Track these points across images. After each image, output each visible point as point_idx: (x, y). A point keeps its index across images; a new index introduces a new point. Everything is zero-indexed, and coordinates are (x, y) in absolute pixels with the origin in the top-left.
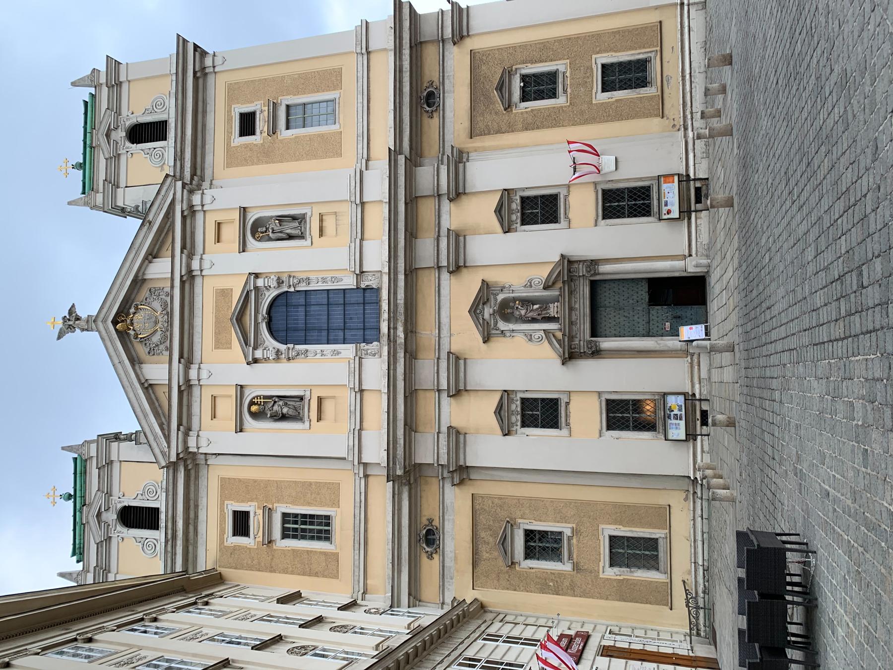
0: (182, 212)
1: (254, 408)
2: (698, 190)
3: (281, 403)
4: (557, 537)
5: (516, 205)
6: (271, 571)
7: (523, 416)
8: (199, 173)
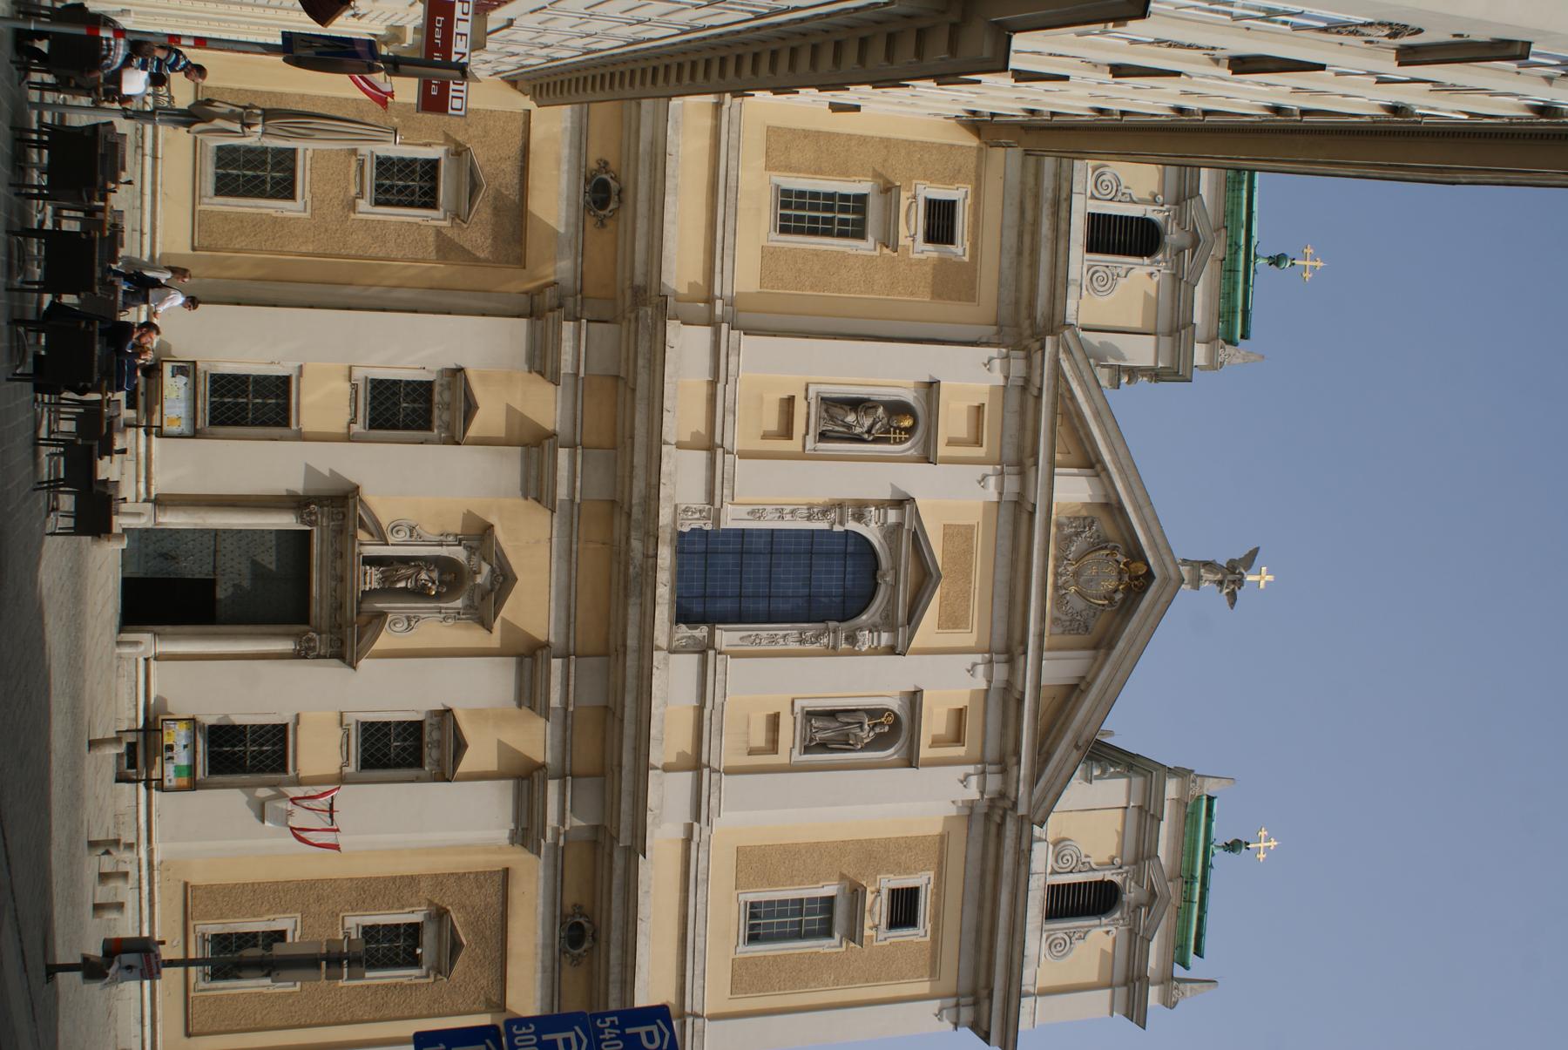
0: (1019, 763)
1: (907, 423)
2: (132, 764)
3: (858, 430)
4: (384, 197)
5: (430, 755)
6: (888, 139)
7: (429, 400)
8: (993, 829)
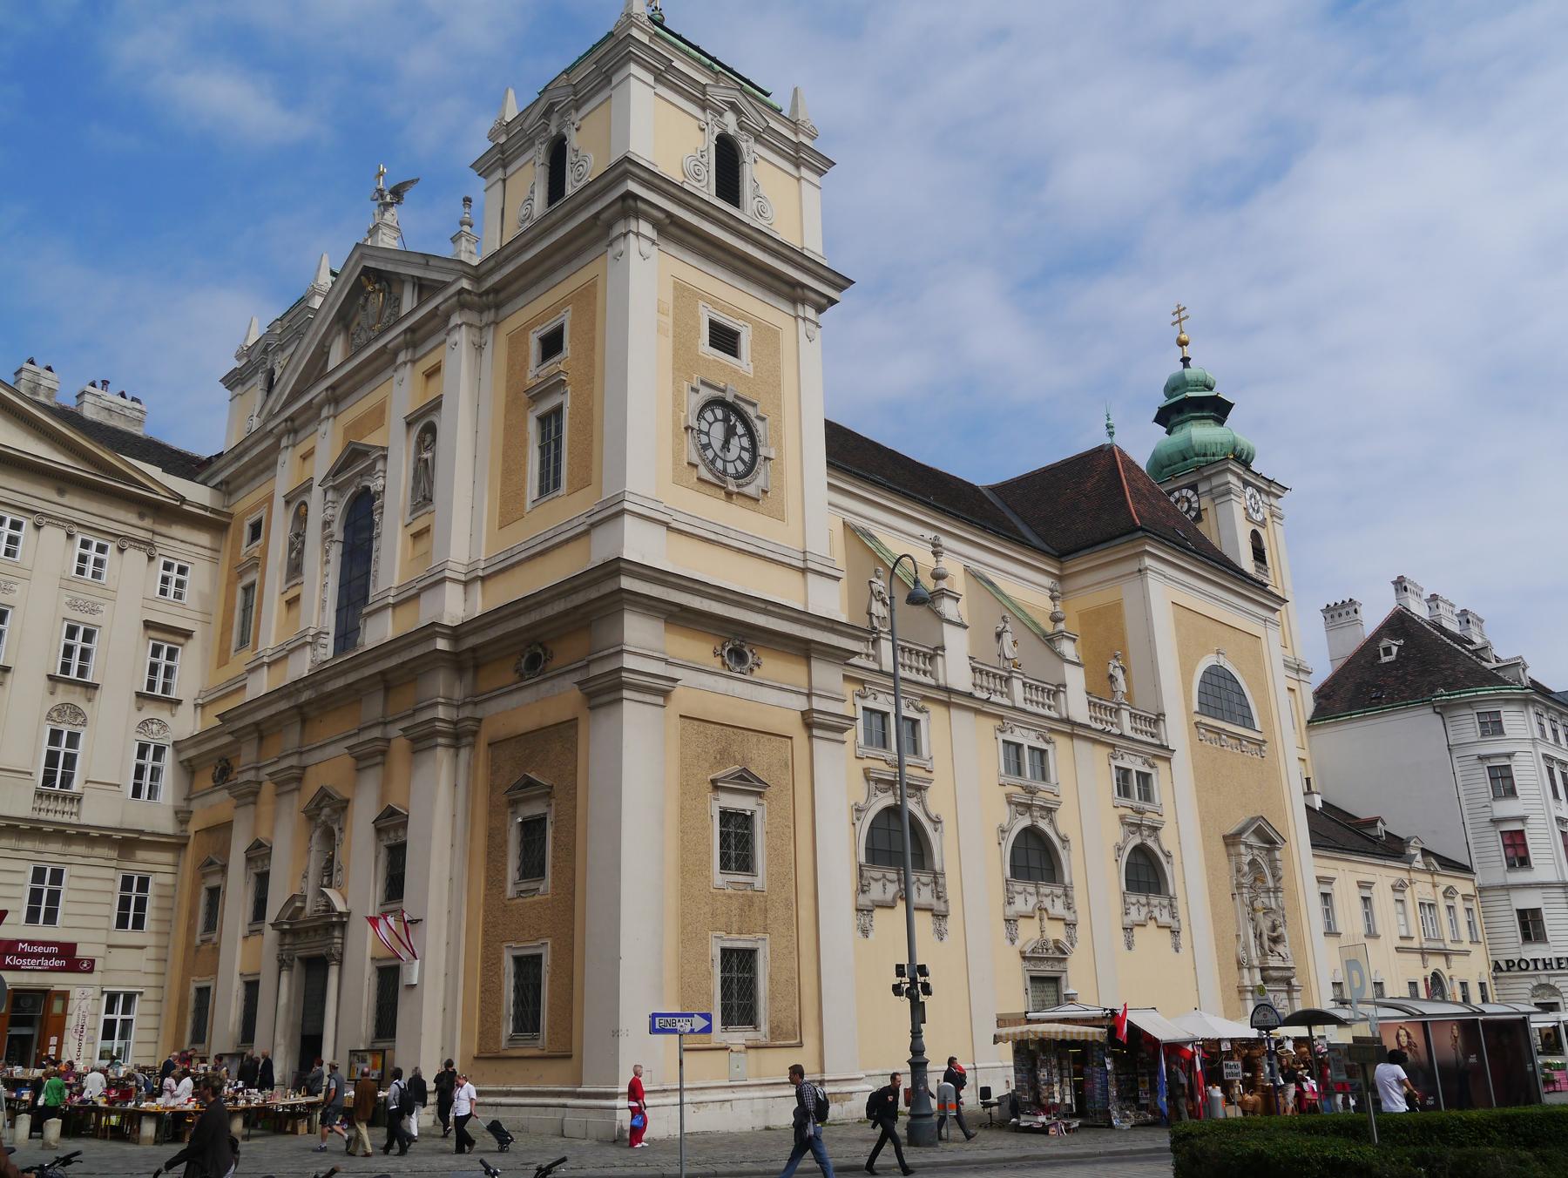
8: (502, 296)
